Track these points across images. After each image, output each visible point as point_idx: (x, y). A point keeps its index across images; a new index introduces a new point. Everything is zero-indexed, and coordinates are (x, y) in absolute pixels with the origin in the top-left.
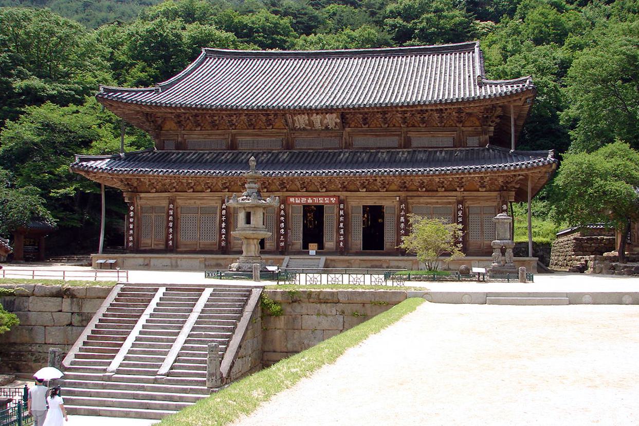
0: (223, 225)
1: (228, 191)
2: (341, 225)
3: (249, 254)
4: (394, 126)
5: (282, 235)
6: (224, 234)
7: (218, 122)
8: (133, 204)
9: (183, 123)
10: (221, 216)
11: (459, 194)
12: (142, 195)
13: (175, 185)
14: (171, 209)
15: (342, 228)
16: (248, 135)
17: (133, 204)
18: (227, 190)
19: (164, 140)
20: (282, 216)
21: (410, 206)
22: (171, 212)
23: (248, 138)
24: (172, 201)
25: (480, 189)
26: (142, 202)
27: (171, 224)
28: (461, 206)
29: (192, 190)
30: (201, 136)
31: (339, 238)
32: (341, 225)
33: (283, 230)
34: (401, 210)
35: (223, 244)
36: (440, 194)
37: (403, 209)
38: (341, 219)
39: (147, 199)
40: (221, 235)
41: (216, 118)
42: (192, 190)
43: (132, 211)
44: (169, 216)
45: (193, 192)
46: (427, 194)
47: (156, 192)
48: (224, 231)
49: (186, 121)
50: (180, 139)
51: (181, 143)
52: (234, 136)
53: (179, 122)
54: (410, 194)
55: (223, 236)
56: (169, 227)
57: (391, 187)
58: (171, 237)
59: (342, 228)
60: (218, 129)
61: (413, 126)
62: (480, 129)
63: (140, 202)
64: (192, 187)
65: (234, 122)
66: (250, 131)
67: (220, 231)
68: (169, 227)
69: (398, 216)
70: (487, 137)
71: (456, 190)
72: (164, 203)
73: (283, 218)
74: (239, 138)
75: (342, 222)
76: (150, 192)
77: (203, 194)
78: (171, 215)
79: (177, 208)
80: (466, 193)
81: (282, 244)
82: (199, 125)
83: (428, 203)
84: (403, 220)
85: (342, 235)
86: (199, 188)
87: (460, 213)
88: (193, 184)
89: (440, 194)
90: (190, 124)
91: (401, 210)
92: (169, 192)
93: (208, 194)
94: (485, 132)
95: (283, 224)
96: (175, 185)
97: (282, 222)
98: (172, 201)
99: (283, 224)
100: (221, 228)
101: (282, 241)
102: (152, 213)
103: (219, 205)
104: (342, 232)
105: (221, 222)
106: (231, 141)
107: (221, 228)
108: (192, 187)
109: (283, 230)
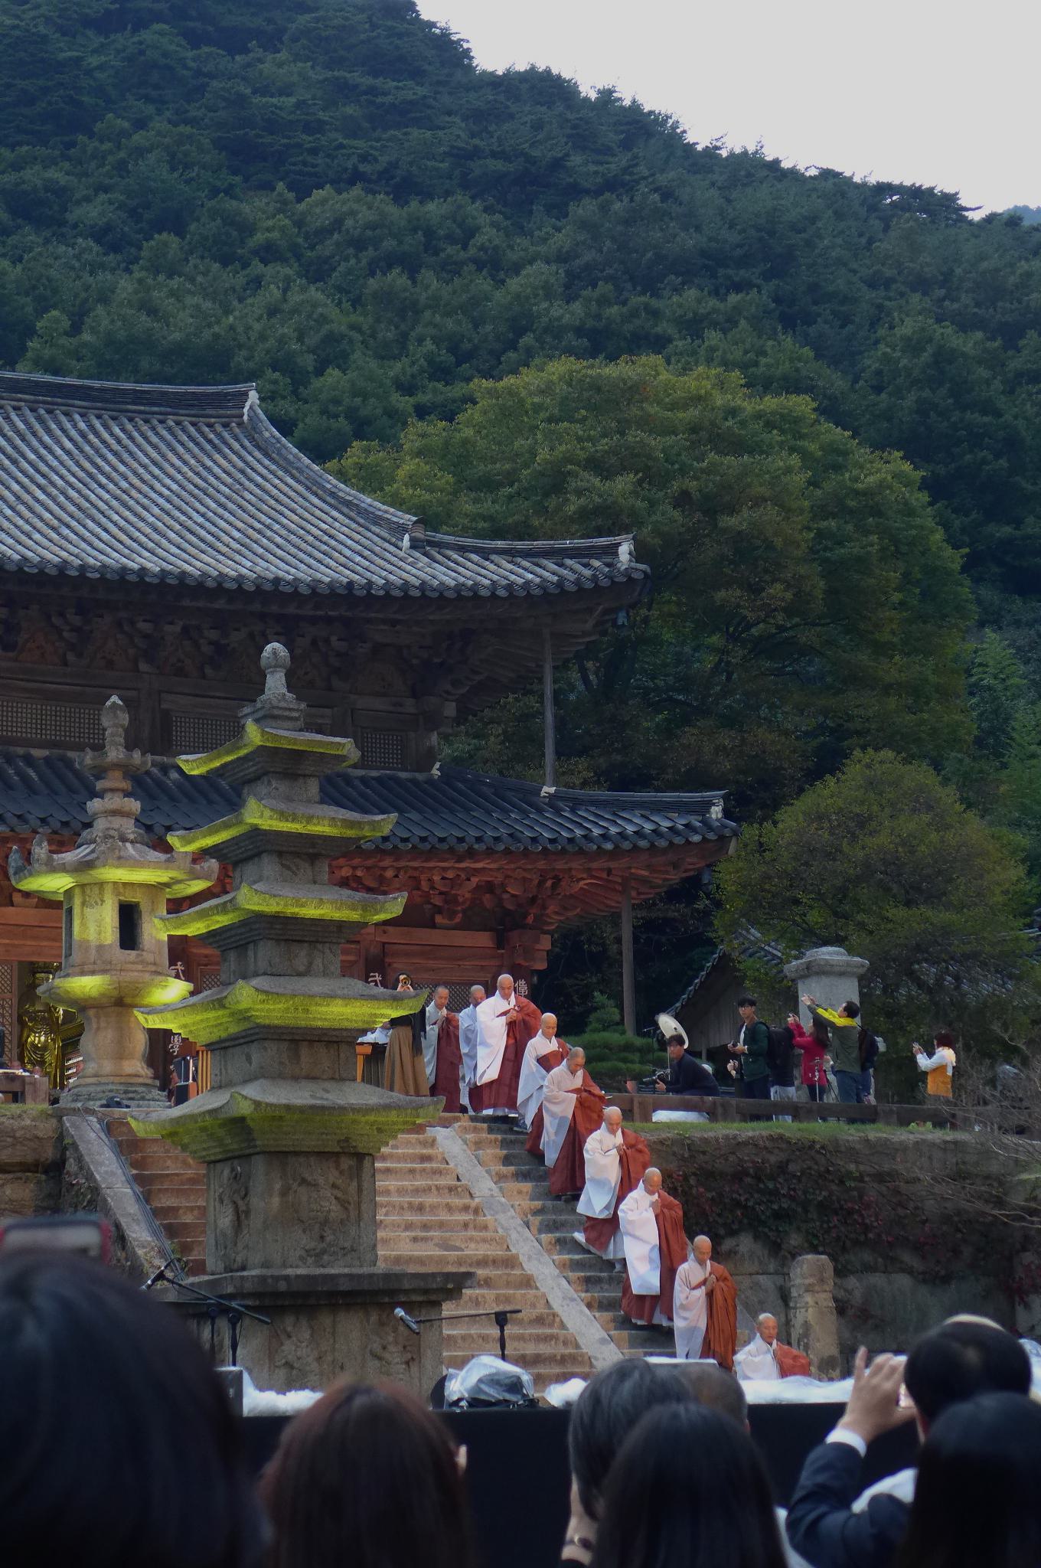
4: (110, 664)
25: (438, 919)
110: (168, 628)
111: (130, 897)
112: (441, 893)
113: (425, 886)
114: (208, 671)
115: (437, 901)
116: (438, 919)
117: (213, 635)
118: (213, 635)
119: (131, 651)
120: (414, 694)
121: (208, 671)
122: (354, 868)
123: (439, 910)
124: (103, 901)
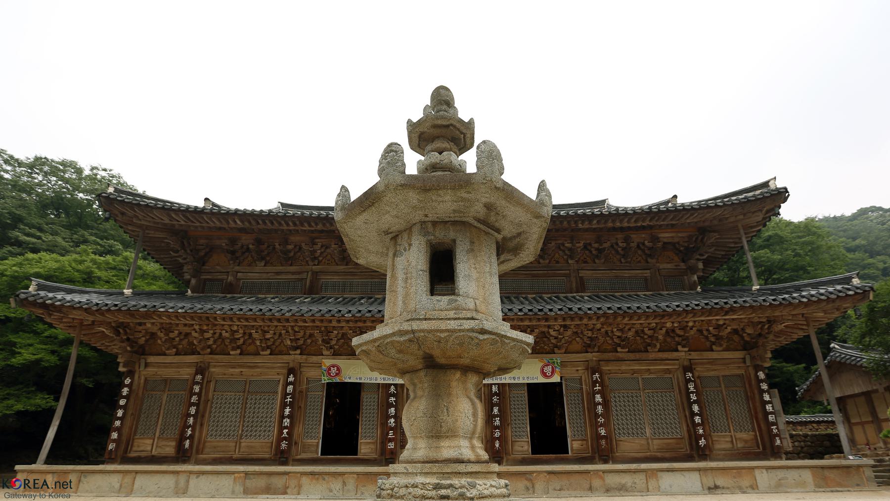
0: (287, 411)
1: (300, 354)
2: (496, 410)
3: (448, 450)
4: (557, 262)
5: (392, 429)
6: (286, 428)
7: (292, 254)
8: (131, 373)
9: (238, 254)
10: (285, 395)
11: (682, 354)
12: (151, 359)
13: (211, 342)
14: (197, 383)
15: (497, 416)
16: (336, 273)
17: (131, 373)
18: (298, 352)
19: (205, 279)
20: (393, 395)
21: (606, 378)
22: (197, 389)
23: (336, 279)
24: (201, 370)
25: (714, 347)
26: (151, 370)
27: (193, 410)
28: (690, 375)
29: (239, 351)
30: (265, 276)
31: (492, 433)
32: (496, 410)
33: (392, 420)
34: (594, 383)
35: (284, 445)
36: (652, 356)
37: (596, 382)
38: (495, 399)
39: (158, 365)
40: (281, 428)
41: (290, 247)
42: (239, 351)
43: (127, 386)
44: (192, 394)
45: (240, 354)
46: (632, 356)
47: (177, 354)
48: (286, 422)
49: (243, 253)
50: (230, 278)
51: (231, 284)
52: (315, 274)
53: (233, 253)
54: (606, 356)
55: (285, 431)
56: (189, 415)
57: (571, 346)
58: (189, 432)
59: (497, 416)
60: (291, 265)
61: (586, 262)
62: (683, 266)
63: (144, 373)
64: (238, 347)
65: (318, 254)
66: (341, 268)
67: (281, 422)
68: (189, 415)
69: (588, 394)
70: (695, 278)
71: (677, 350)
72: (186, 373)
73: (393, 399)
74: (325, 279)
75: (496, 405)
76: (165, 354)
77: (257, 359)
78: (195, 394)
79: (209, 382)
80: (694, 355)
81: (391, 445)
82: (263, 259)
83: (634, 372)
84: (600, 400)
85: (497, 427)
86: (251, 348)
87: (691, 387)
88: (242, 341)
89: (652, 356)
90: (250, 258)
91: (594, 383)
92: (199, 354)
93: (265, 358)
94: (693, 270)
95: (392, 410)
96: (211, 342)
97: (391, 405)
98: (201, 370)
99: (392, 410)
100: (282, 417)
101: (390, 440)
102: (164, 391)
103: (282, 378)
104: (497, 422)
105: (284, 405)
106: (311, 282)
107: (282, 417)
108: (238, 347)
109: (392, 420)
110: (578, 245)
111: (442, 235)
112: (714, 336)
113: (705, 333)
114: (597, 261)
115: (713, 339)
116: (714, 347)
117: (596, 245)
118: (596, 245)
119: (565, 257)
120: (683, 261)
121: (597, 261)
122: (673, 323)
123: (714, 343)
124: (410, 245)
